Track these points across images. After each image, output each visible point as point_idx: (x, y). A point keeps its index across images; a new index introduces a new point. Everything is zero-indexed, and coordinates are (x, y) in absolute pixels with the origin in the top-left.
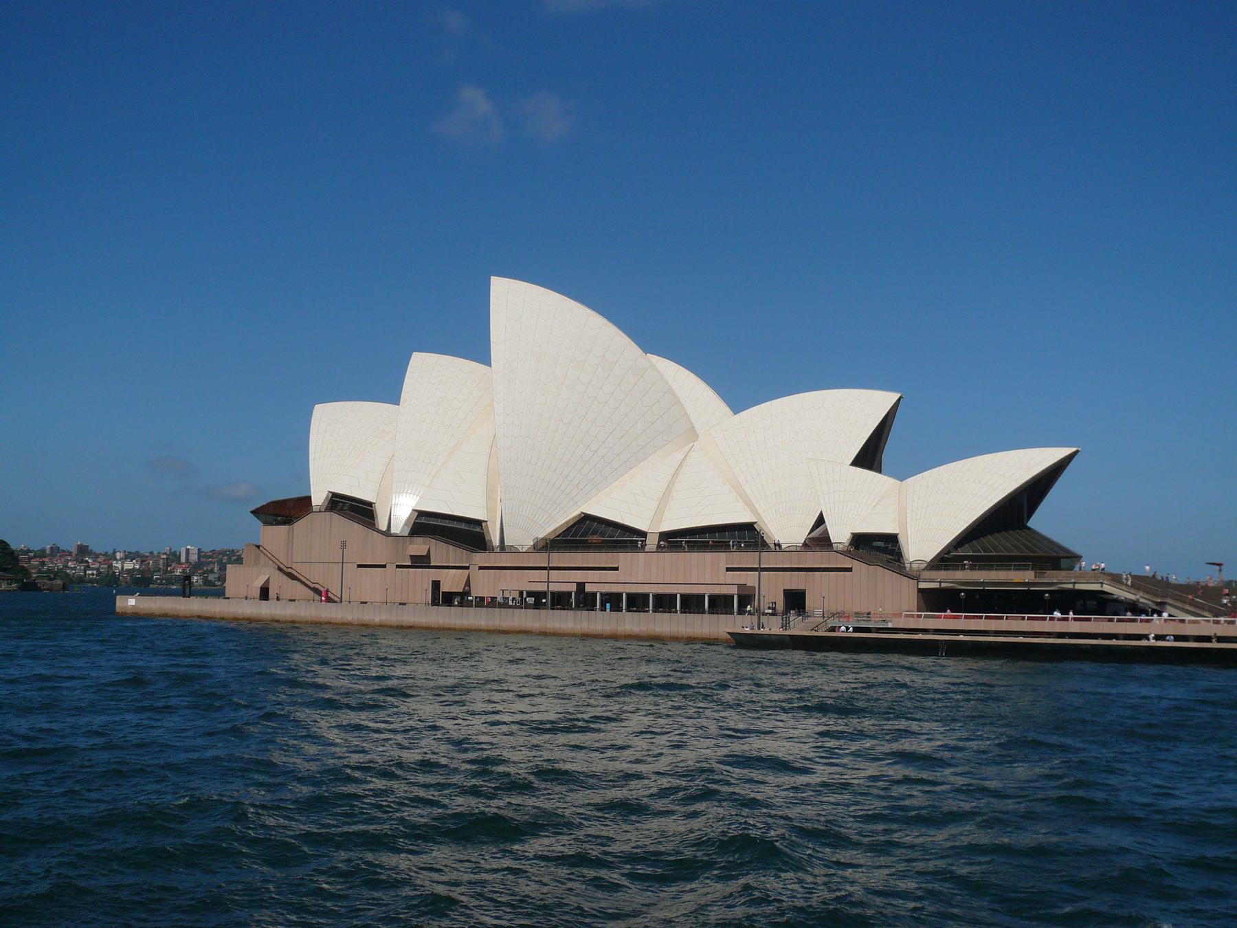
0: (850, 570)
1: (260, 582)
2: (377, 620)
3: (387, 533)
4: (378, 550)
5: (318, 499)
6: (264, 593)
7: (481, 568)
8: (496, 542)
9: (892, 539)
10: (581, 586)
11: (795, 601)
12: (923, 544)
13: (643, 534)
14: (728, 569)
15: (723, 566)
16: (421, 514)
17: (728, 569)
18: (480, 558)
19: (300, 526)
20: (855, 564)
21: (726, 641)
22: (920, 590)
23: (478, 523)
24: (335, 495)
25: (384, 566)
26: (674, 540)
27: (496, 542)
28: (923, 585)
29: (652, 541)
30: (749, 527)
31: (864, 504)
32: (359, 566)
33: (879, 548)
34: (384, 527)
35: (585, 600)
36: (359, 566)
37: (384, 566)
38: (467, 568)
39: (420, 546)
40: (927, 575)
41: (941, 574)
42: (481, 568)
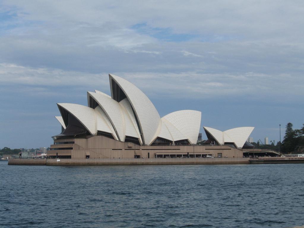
0: (231, 149)
2: (151, 162)
4: (120, 146)
6: (88, 157)
7: (142, 149)
10: (188, 153)
11: (220, 155)
12: (240, 144)
13: (171, 142)
14: (206, 149)
15: (205, 149)
16: (127, 137)
17: (206, 149)
18: (142, 147)
19: (90, 140)
20: (231, 148)
21: (249, 162)
22: (244, 153)
23: (137, 139)
24: (98, 131)
25: (122, 149)
28: (244, 152)
29: (174, 143)
30: (187, 140)
32: (113, 149)
34: (118, 140)
35: (179, 156)
36: (113, 149)
37: (122, 149)
38: (139, 149)
39: (130, 144)
40: (243, 150)
41: (246, 150)
42: (142, 149)
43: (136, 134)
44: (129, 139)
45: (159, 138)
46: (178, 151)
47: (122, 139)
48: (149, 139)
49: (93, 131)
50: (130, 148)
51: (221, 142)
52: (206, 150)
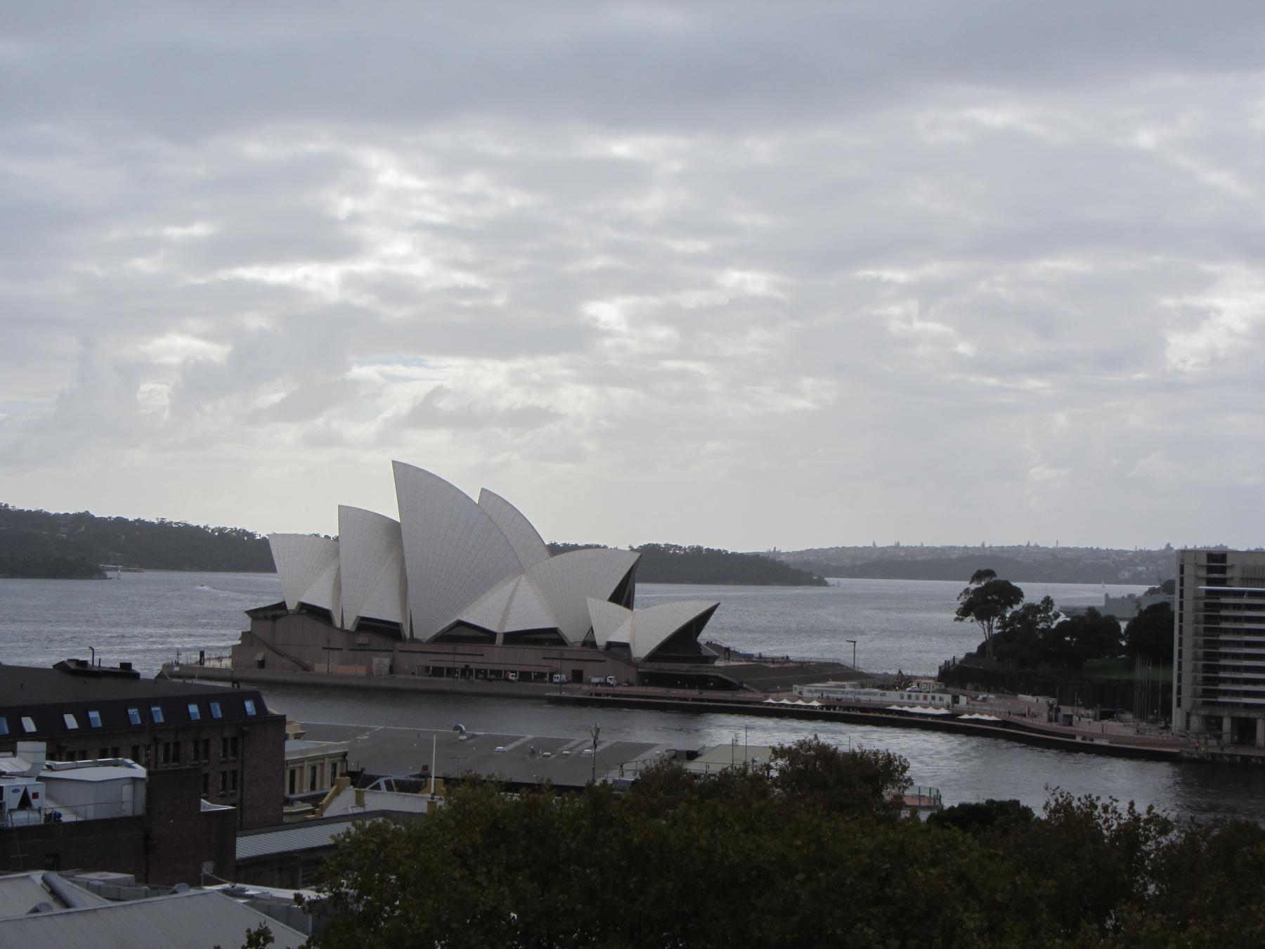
1: (259, 657)
3: (342, 630)
5: (291, 606)
6: (262, 664)
8: (408, 636)
9: (626, 646)
16: (363, 619)
18: (399, 646)
23: (397, 624)
26: (514, 638)
27: (408, 636)
29: (499, 640)
30: (554, 630)
31: (615, 626)
33: (619, 650)
34: (338, 625)
39: (362, 639)
43: (390, 613)
44: (366, 625)
45: (460, 624)
46: (478, 659)
47: (349, 625)
48: (427, 626)
49: (291, 606)
50: (363, 648)
51: (601, 641)
52: (544, 662)
